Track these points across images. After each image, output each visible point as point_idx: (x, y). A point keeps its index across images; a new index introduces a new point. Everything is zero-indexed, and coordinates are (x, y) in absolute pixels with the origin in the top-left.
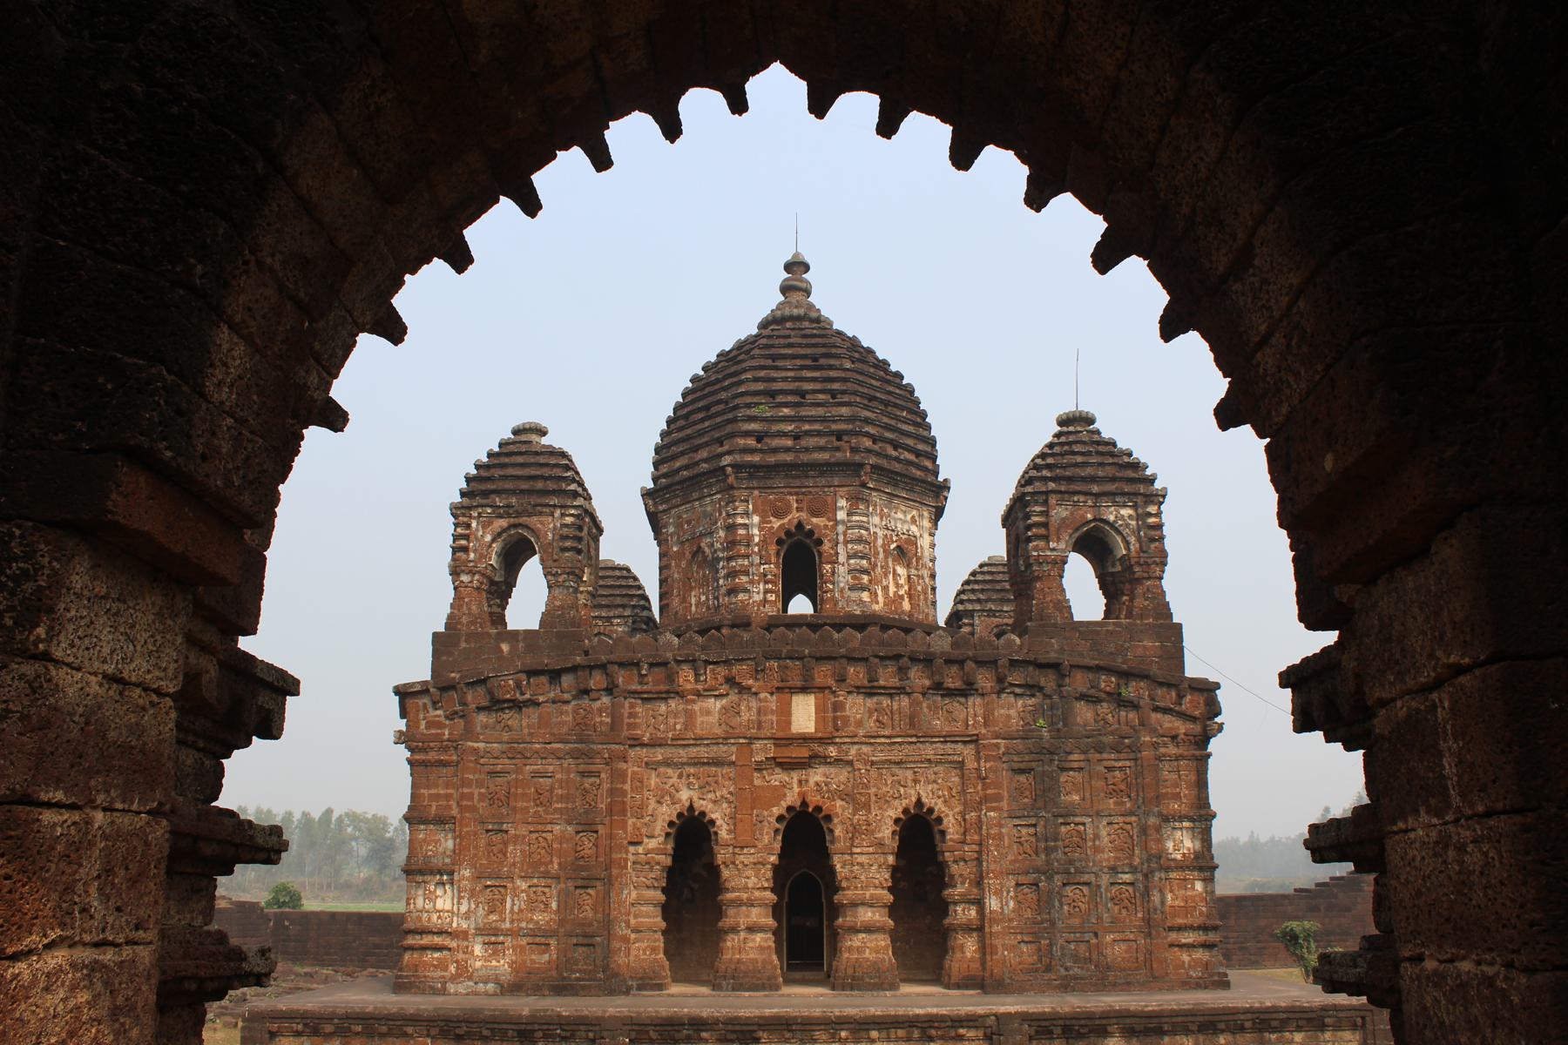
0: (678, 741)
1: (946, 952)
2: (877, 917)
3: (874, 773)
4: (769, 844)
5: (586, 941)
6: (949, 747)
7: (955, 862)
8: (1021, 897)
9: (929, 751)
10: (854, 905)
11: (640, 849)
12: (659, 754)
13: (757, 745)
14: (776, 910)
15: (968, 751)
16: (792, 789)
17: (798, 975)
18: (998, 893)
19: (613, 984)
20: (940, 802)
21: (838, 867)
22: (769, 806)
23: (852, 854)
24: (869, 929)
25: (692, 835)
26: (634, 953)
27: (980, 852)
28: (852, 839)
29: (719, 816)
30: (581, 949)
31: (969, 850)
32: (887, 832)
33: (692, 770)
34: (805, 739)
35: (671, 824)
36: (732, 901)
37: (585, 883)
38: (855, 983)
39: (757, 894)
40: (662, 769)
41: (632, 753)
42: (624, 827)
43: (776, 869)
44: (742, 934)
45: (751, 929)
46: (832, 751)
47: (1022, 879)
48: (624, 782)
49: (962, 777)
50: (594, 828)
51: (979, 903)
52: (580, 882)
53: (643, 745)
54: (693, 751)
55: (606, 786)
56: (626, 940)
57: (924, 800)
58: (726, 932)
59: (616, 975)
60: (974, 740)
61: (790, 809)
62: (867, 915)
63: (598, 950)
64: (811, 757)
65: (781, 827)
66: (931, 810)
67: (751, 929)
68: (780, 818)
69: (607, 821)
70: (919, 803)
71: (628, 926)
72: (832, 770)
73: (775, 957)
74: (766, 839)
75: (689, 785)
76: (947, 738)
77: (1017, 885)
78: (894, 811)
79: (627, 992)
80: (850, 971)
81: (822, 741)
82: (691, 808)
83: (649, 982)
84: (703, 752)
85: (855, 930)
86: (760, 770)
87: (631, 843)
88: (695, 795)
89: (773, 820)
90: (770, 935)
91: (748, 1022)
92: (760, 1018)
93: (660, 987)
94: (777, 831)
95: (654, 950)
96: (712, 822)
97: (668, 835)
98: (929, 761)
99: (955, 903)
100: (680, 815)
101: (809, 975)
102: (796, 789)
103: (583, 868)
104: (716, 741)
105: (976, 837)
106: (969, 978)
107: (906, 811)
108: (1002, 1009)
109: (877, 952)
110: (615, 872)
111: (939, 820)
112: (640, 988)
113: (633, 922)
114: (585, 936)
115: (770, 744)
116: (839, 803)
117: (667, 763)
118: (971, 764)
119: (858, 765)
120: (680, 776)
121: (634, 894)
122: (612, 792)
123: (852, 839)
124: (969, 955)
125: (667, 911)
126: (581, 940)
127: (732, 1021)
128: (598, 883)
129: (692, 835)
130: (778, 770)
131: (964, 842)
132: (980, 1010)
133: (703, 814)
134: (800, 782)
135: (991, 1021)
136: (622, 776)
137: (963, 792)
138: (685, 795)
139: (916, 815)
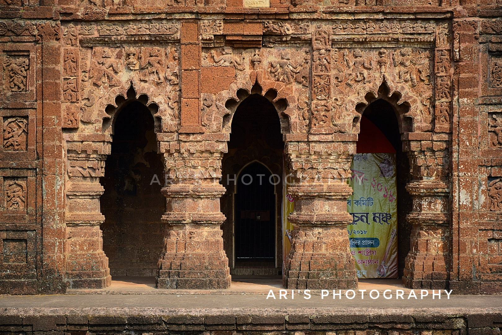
0: (116, 18)
1: (409, 250)
2: (335, 211)
3: (334, 53)
4: (218, 132)
5: (17, 236)
6: (419, 27)
7: (422, 152)
8: (493, 191)
9: (397, 30)
10: (310, 198)
11: (75, 136)
12: (94, 32)
13: (205, 22)
14: (225, 203)
15: (441, 30)
16: (243, 71)
17: (247, 271)
18: (468, 187)
19: (46, 281)
20: (407, 86)
21: (293, 157)
22: (217, 90)
23: (308, 142)
24: (325, 224)
25: (133, 119)
26: (69, 248)
27: (449, 143)
28: (309, 126)
29: (161, 98)
30: (12, 245)
31: (438, 140)
32: (348, 119)
33: (132, 49)
34: (258, 16)
35: (109, 109)
36: (177, 193)
37: (15, 173)
38: (310, 281)
39: (205, 185)
40: (98, 49)
41: (64, 30)
42: (57, 111)
43: (226, 159)
44: (188, 228)
45: (196, 223)
46: (289, 29)
47: (495, 172)
48: (57, 62)
49: (432, 59)
50: (23, 112)
51: (448, 199)
52: (9, 173)
53: (77, 21)
54: (133, 28)
55: (36, 67)
56: (60, 233)
57: (390, 83)
58: (170, 225)
59: (51, 272)
60: (448, 19)
61: (241, 92)
62: (322, 209)
63: (31, 245)
64: (264, 35)
65: (231, 112)
66: (397, 96)
67: (196, 223)
68: (230, 103)
69: (38, 105)
70: (384, 87)
71: (62, 216)
72: (289, 51)
73: (223, 253)
74: (214, 125)
75: (128, 67)
76: (417, 16)
77: (490, 178)
78: (357, 96)
79: (63, 291)
80: (305, 268)
81: (278, 17)
82: (131, 91)
83: (85, 279)
84: (144, 29)
85: (309, 225)
86: (207, 49)
87: (65, 130)
88: (135, 76)
89: (222, 104)
90: (218, 229)
91: (194, 321)
92: (206, 317)
93: (99, 284)
94: (226, 117)
95: (92, 245)
96: (155, 107)
97: (106, 120)
98: (397, 41)
99: (420, 197)
100: (119, 99)
101: (260, 271)
102: (248, 70)
103: (12, 157)
104: (157, 17)
105: (446, 126)
106: (432, 277)
107: (369, 96)
108: (473, 311)
109: (334, 248)
110: (47, 160)
111: (406, 106)
112: (76, 285)
113: (68, 214)
114: (15, 231)
115: (219, 21)
116: (295, 86)
117: (105, 41)
118: (443, 45)
119: (316, 45)
120: (119, 56)
121: (69, 185)
122: (42, 73)
123: (309, 126)
124: (433, 252)
125: (105, 202)
126: (11, 235)
127: (175, 321)
128: (30, 174)
129: (133, 119)
130: (228, 50)
131: (432, 131)
132: (449, 311)
133: (145, 97)
134: (253, 63)
135: (460, 324)
136: (54, 55)
137: (433, 76)
138: (124, 77)
139: (379, 100)
